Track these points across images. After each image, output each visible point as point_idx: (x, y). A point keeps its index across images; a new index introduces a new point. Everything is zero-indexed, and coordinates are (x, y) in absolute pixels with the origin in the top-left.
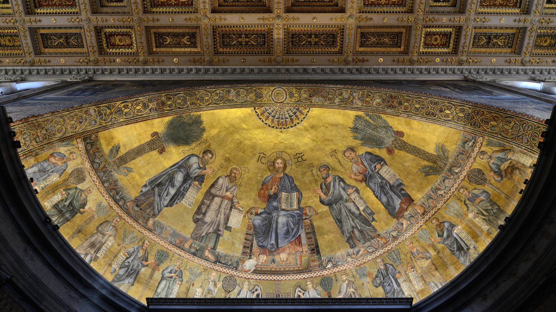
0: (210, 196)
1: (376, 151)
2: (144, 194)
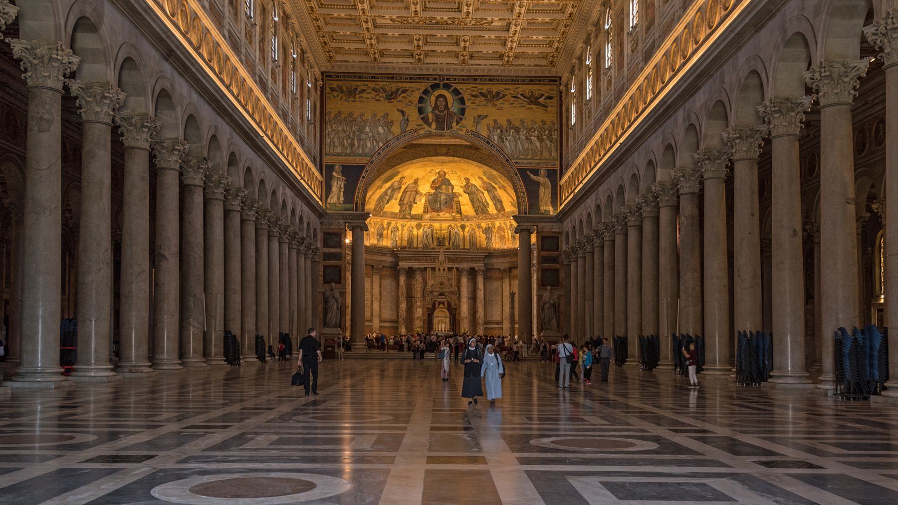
0: (405, 192)
1: (493, 184)
2: (376, 205)
